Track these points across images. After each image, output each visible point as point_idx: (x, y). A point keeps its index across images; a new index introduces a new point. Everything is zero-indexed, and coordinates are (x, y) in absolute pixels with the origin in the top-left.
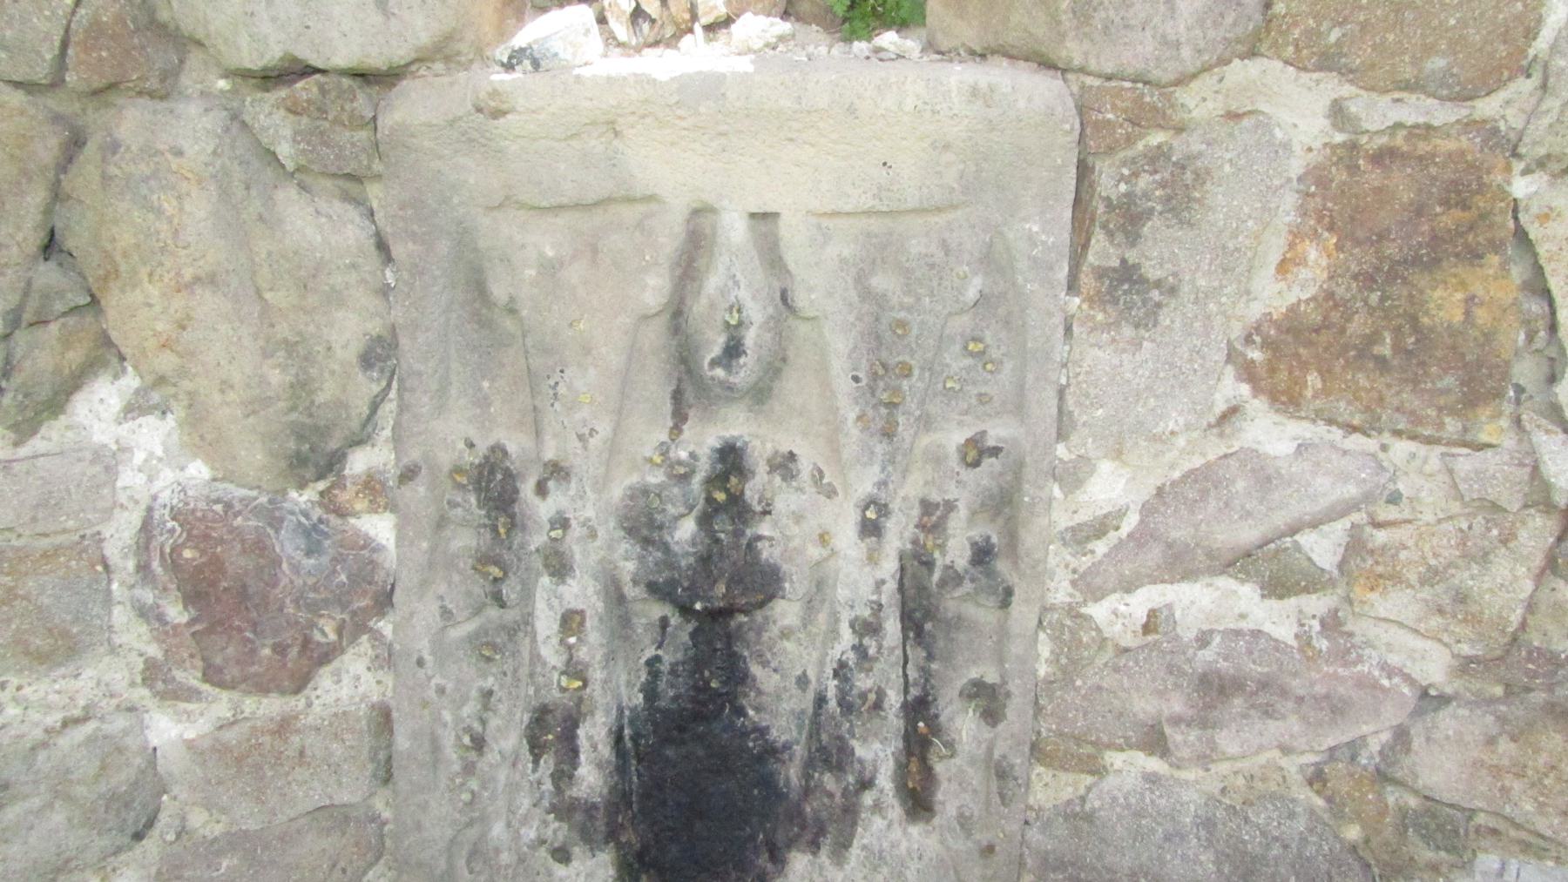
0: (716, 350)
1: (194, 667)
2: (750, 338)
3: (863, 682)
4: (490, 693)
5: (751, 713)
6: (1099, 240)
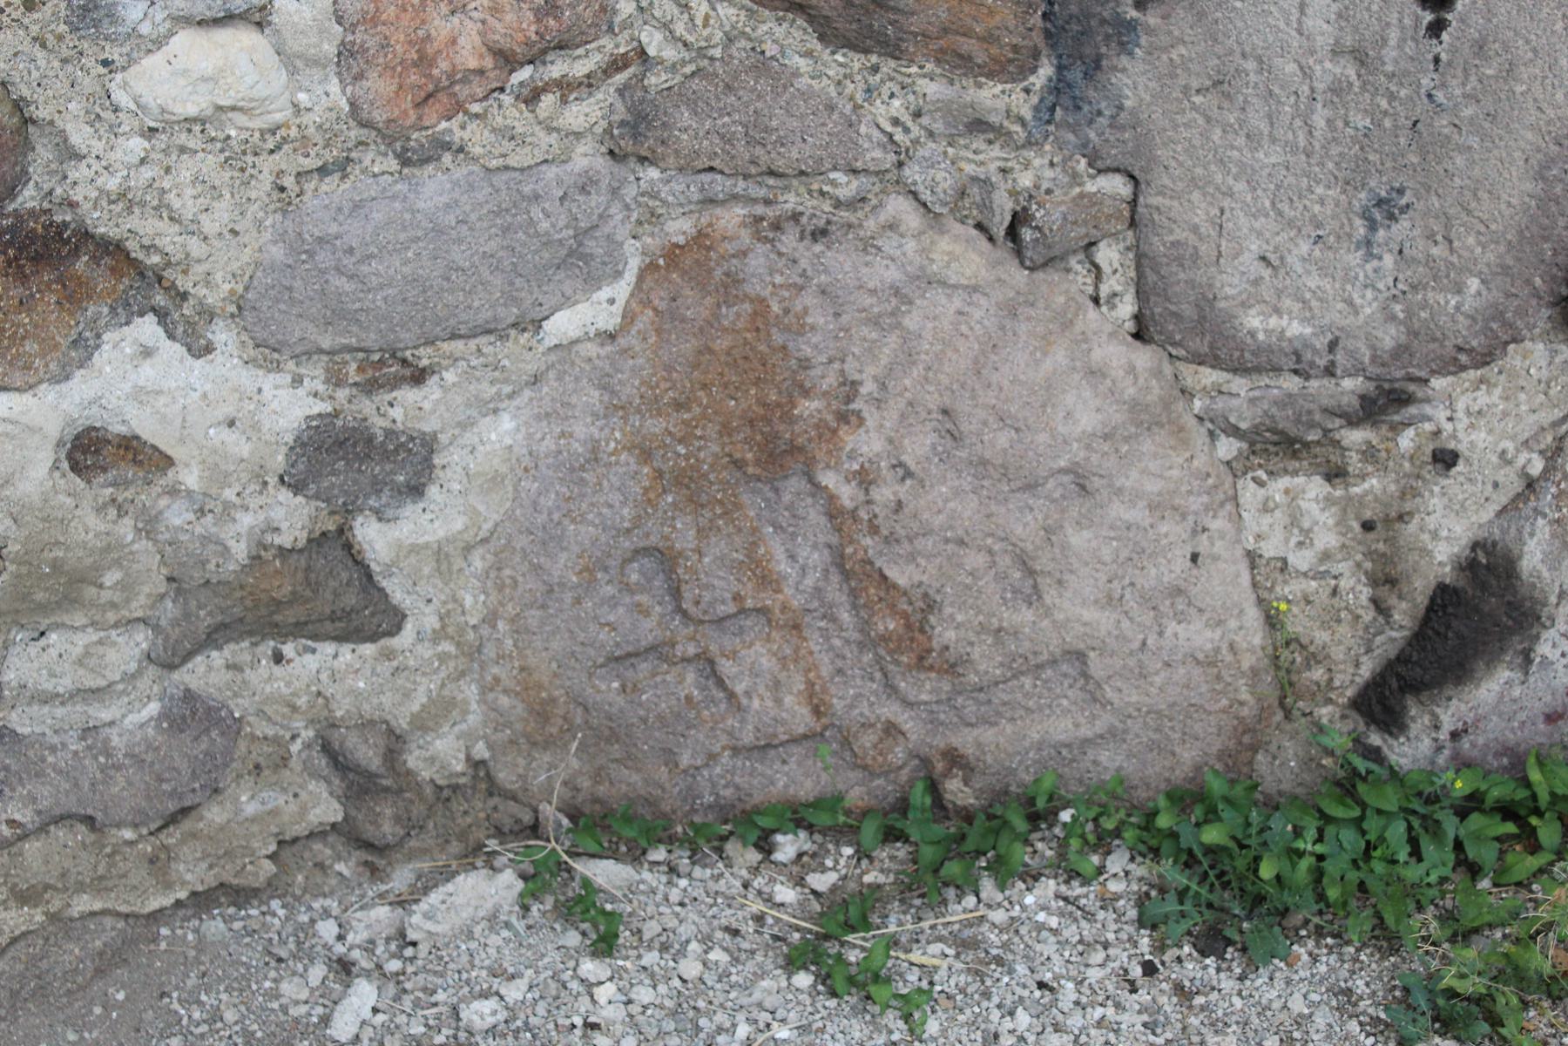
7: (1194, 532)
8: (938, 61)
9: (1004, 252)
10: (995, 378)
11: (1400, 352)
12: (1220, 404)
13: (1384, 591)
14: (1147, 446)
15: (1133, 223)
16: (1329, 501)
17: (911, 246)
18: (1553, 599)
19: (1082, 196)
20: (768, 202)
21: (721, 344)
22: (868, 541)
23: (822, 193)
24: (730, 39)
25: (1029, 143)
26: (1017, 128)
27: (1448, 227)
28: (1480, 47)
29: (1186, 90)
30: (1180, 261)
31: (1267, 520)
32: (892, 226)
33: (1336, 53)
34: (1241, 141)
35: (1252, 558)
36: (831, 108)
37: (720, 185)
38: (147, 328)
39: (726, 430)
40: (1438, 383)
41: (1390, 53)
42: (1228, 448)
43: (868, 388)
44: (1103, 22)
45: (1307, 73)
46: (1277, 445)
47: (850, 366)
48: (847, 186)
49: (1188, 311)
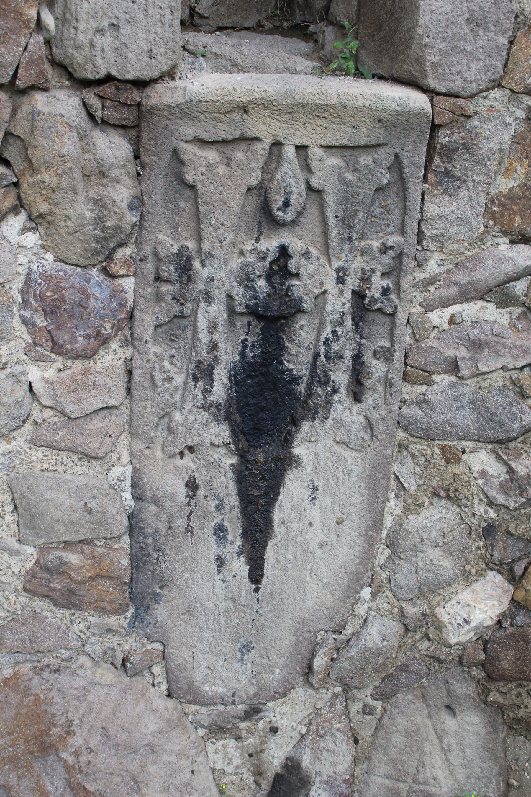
0: (280, 203)
1: (47, 346)
2: (293, 199)
3: (336, 347)
4: (174, 356)
5: (286, 363)
6: (437, 160)
7: (192, 763)
8: (95, 611)
9: (121, 672)
10: (120, 715)
11: (256, 695)
12: (198, 717)
13: (258, 777)
14: (174, 734)
15: (164, 658)
16: (237, 748)
17: (88, 672)
18: (314, 776)
19: (146, 651)
20: (38, 661)
21: (24, 711)
22: (79, 776)
23: (57, 657)
24: (23, 608)
25: (127, 635)
26: (123, 630)
27: (267, 653)
28: (271, 595)
29: (178, 614)
30: (180, 670)
31: (217, 756)
32: (81, 667)
33: (225, 600)
34: (197, 630)
35: (213, 769)
36: (59, 628)
37: (21, 657)
39: (26, 741)
40: (269, 704)
41: (243, 599)
42: (201, 732)
43: (76, 722)
44: (149, 594)
45: (217, 606)
46: (218, 730)
47: (70, 715)
48: (65, 654)
49: (184, 686)
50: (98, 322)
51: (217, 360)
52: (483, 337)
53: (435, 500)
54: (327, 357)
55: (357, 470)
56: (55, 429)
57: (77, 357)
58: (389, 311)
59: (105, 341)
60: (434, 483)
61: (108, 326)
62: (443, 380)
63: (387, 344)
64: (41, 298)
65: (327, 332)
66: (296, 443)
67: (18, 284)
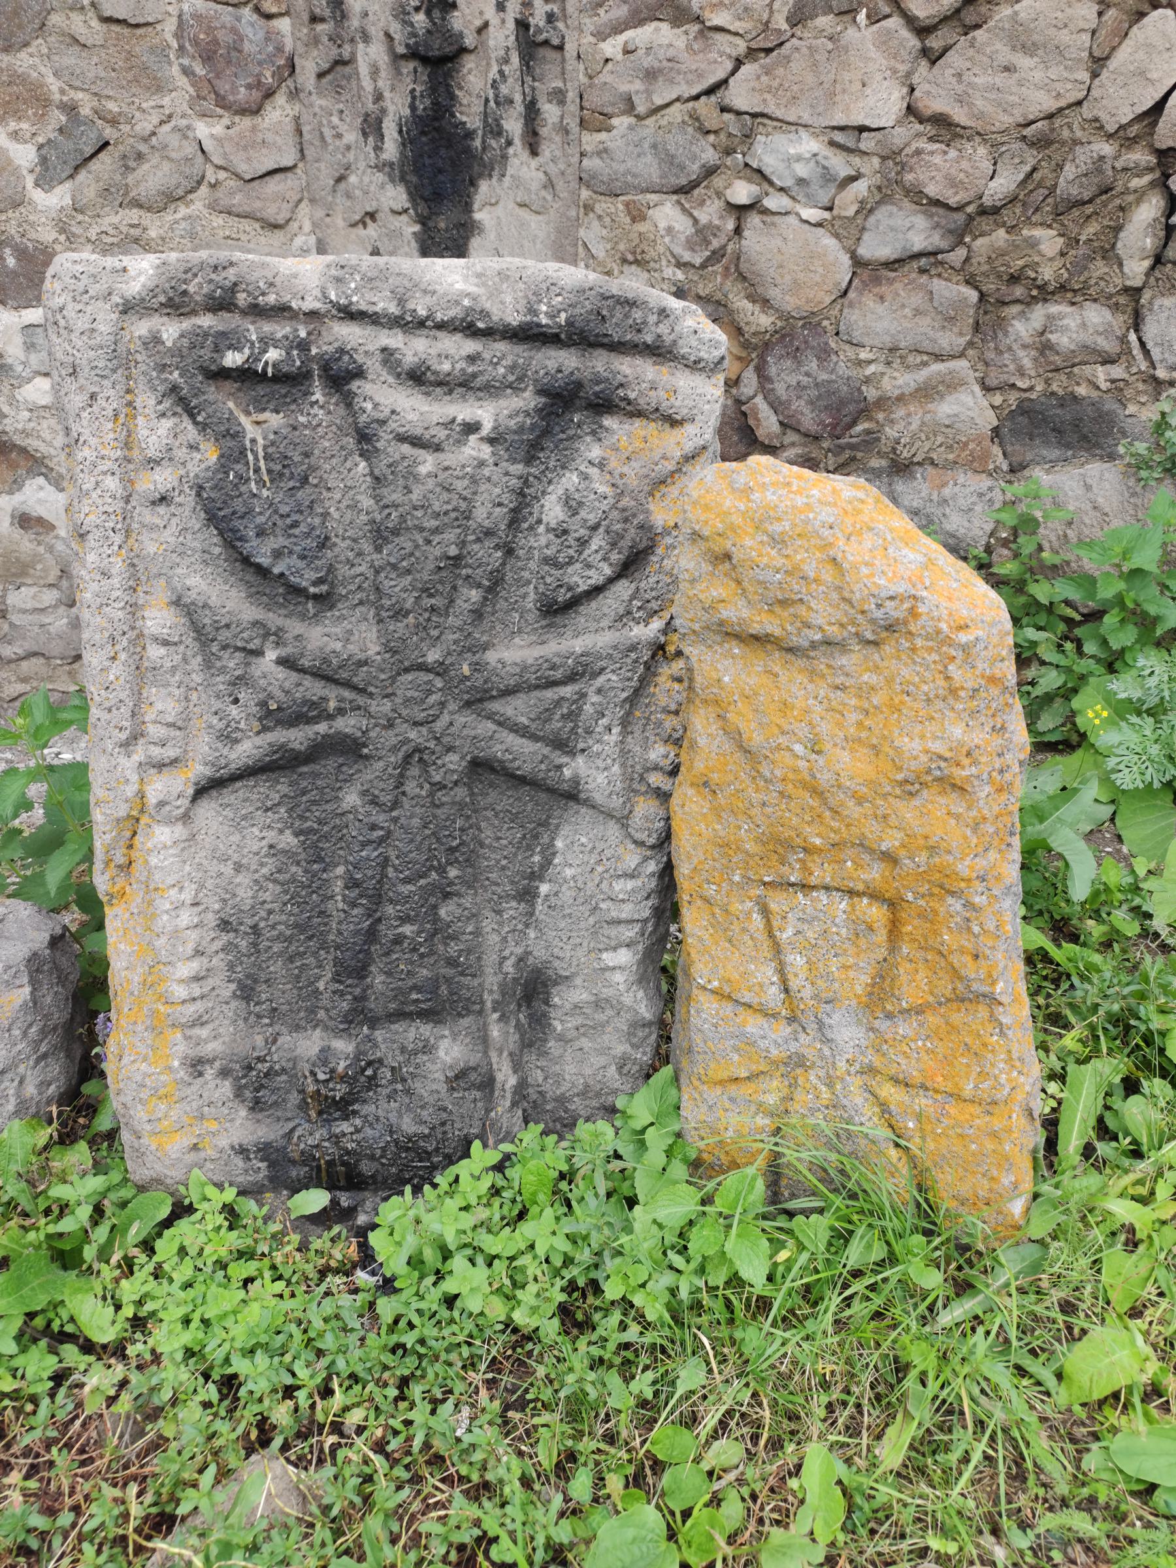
3: (504, 90)
38: (41, 480)
50: (257, 70)
51: (383, 111)
52: (656, 65)
53: (626, 268)
54: (497, 103)
55: (541, 235)
56: (232, 194)
57: (243, 111)
58: (556, 41)
59: (269, 94)
60: (622, 247)
61: (268, 74)
62: (621, 123)
63: (561, 85)
64: (196, 42)
65: (493, 73)
66: (476, 207)
67: (170, 26)
